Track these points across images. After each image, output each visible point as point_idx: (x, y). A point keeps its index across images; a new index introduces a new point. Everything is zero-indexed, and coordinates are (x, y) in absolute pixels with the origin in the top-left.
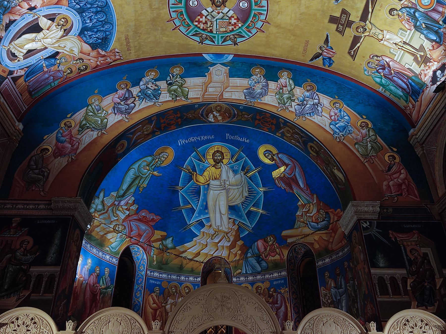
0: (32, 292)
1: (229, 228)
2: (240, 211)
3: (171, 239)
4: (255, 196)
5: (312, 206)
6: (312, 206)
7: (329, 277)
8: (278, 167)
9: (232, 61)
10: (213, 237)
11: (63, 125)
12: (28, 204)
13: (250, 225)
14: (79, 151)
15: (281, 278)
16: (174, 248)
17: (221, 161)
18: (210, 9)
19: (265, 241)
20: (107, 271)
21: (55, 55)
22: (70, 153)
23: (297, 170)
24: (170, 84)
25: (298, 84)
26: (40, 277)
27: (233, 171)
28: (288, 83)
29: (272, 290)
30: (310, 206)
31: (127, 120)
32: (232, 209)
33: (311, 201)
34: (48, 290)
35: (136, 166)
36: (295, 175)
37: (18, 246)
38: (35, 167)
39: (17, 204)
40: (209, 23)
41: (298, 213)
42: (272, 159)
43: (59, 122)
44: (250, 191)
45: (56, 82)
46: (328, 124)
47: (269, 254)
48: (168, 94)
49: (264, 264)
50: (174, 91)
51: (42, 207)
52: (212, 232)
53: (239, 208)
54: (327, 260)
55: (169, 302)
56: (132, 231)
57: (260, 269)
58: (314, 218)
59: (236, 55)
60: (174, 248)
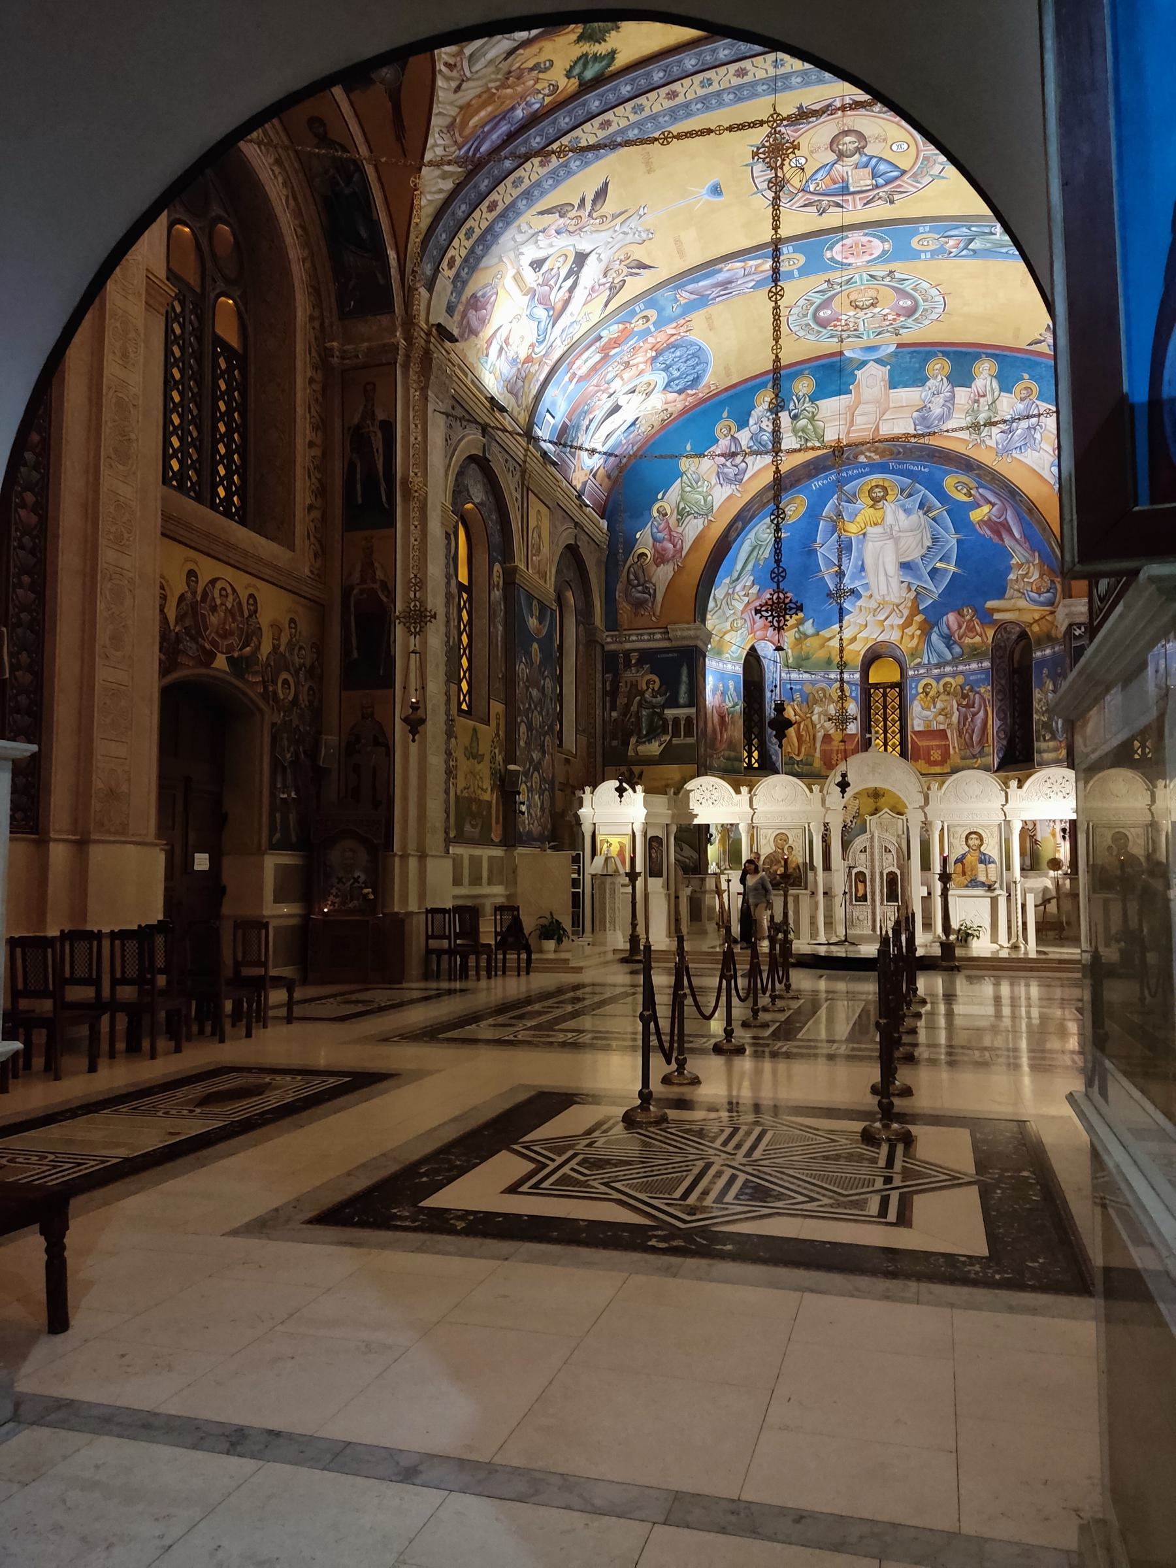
0: (672, 737)
1: (900, 597)
2: (919, 569)
3: (811, 621)
4: (943, 546)
5: (1032, 568)
6: (1032, 568)
7: (1047, 676)
8: (979, 506)
9: (895, 354)
10: (875, 612)
11: (655, 514)
12: (642, 635)
13: (935, 591)
14: (684, 553)
15: (981, 670)
16: (817, 634)
17: (884, 498)
18: (852, 313)
19: (959, 614)
20: (731, 684)
21: (633, 424)
22: (673, 557)
23: (1009, 513)
24: (795, 418)
25: (1006, 387)
26: (676, 720)
27: (905, 510)
28: (988, 388)
29: (967, 688)
30: (1029, 568)
31: (739, 495)
32: (906, 566)
33: (1031, 559)
34: (688, 733)
35: (752, 535)
36: (1006, 519)
37: (645, 687)
38: (636, 582)
39: (630, 635)
40: (851, 325)
41: (1012, 576)
42: (971, 495)
43: (650, 509)
44: (935, 539)
45: (635, 448)
46: (1047, 466)
47: (964, 635)
48: (794, 438)
49: (957, 649)
50: (803, 431)
51: (658, 636)
52: (873, 604)
53: (917, 564)
54: (1048, 651)
55: (816, 712)
56: (754, 623)
57: (949, 657)
58: (1034, 587)
59: (899, 346)
60: (817, 634)
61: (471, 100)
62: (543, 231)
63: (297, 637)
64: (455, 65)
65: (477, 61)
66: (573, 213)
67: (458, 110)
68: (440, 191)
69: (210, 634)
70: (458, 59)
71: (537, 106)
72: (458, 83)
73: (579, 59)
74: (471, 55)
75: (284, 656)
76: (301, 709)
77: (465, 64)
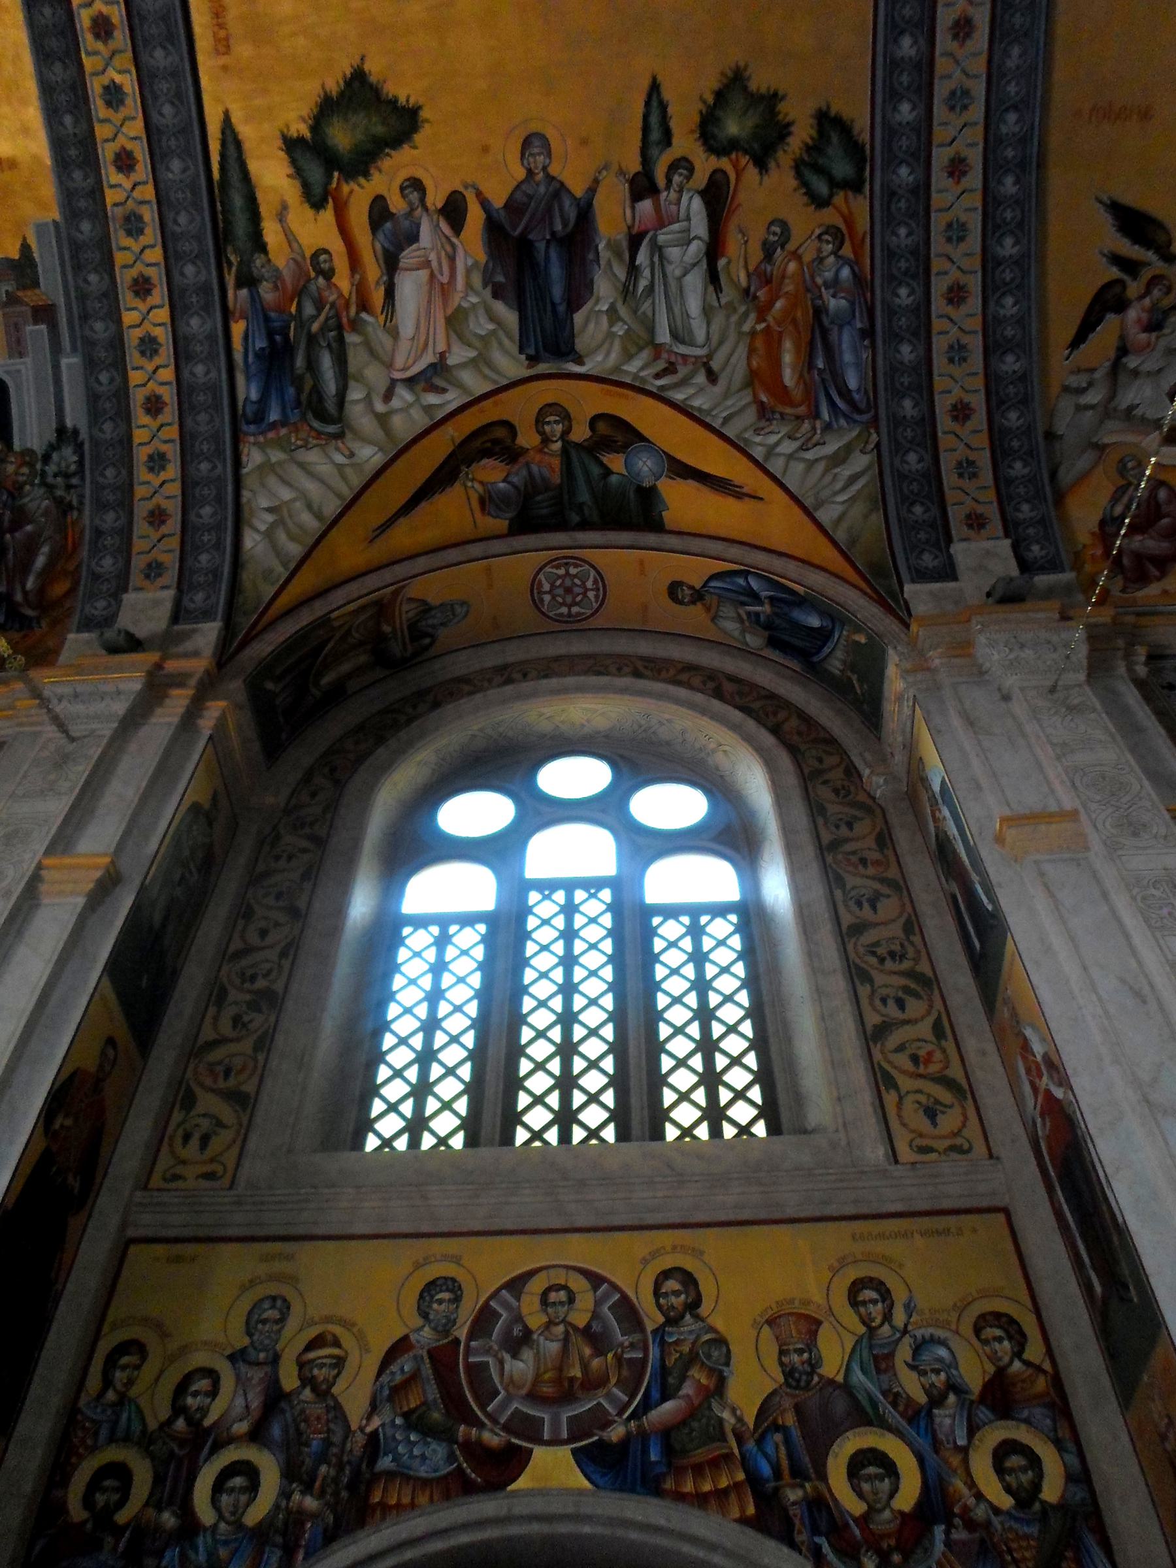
61: (749, 364)
62: (1123, 350)
63: (899, 1317)
64: (672, 364)
65: (691, 332)
66: (1134, 288)
67: (749, 391)
68: (853, 479)
69: (504, 1406)
70: (665, 355)
71: (846, 272)
72: (703, 371)
73: (799, 175)
74: (675, 335)
75: (846, 1388)
76: (970, 1525)
77: (682, 349)
